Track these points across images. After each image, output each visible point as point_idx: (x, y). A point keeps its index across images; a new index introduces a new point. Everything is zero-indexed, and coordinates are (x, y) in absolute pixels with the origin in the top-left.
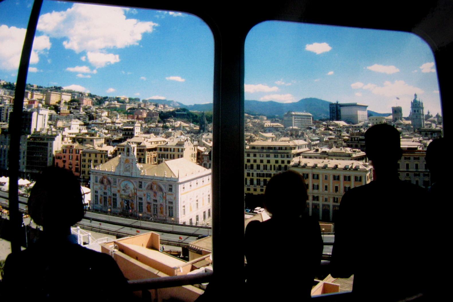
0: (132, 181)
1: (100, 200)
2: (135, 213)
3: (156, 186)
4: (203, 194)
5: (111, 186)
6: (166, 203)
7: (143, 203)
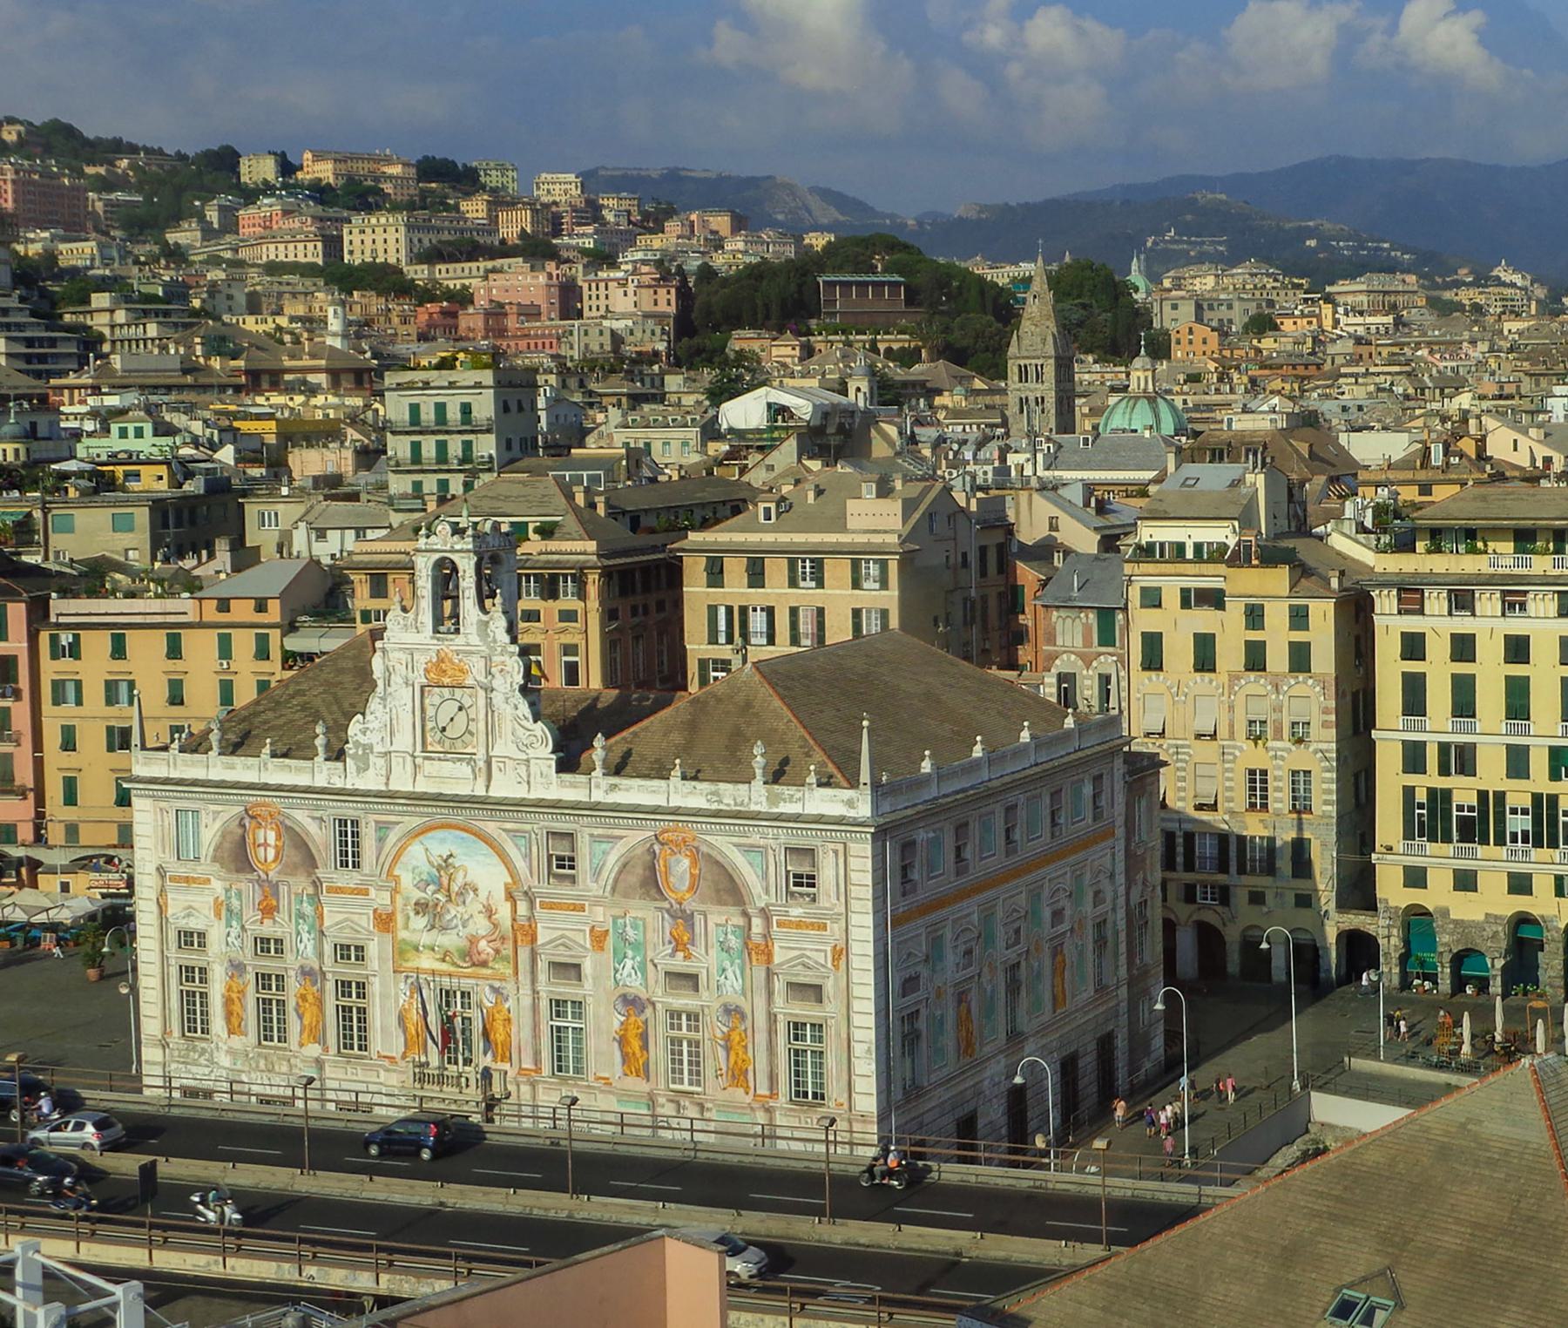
0: (491, 828)
1: (228, 1001)
2: (525, 1089)
3: (686, 862)
4: (1057, 915)
5: (317, 884)
6: (770, 994)
7: (590, 1009)
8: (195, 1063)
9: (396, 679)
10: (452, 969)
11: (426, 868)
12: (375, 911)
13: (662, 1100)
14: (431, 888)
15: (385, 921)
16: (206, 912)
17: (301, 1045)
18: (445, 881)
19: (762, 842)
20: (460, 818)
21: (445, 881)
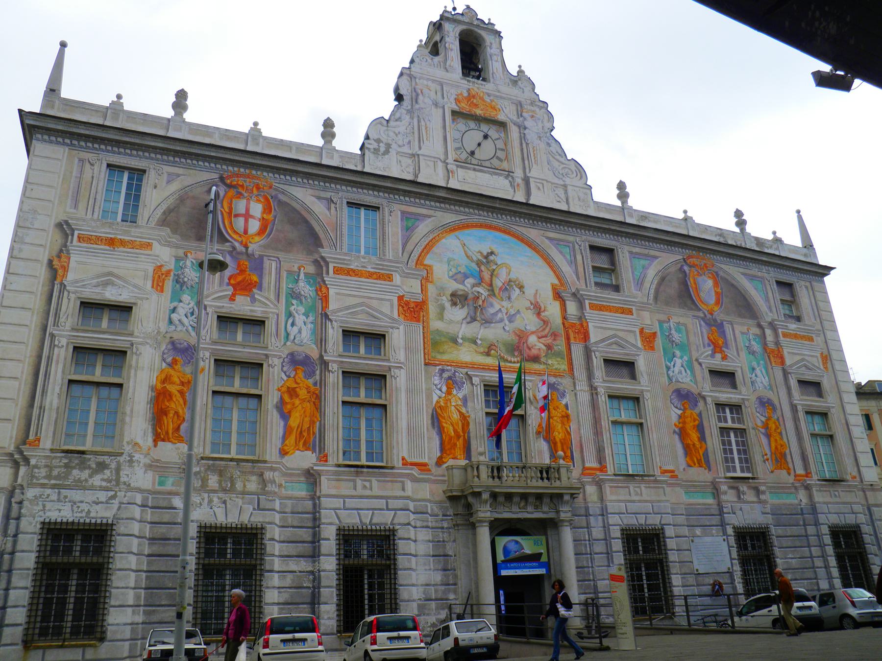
0: (534, 233)
2: (591, 490)
3: (710, 283)
5: (321, 264)
6: (789, 389)
7: (649, 403)
8: (79, 485)
9: (424, 101)
11: (465, 261)
12: (400, 298)
13: (724, 488)
14: (470, 281)
16: (140, 282)
17: (283, 453)
18: (486, 276)
19: (759, 274)
20: (500, 221)
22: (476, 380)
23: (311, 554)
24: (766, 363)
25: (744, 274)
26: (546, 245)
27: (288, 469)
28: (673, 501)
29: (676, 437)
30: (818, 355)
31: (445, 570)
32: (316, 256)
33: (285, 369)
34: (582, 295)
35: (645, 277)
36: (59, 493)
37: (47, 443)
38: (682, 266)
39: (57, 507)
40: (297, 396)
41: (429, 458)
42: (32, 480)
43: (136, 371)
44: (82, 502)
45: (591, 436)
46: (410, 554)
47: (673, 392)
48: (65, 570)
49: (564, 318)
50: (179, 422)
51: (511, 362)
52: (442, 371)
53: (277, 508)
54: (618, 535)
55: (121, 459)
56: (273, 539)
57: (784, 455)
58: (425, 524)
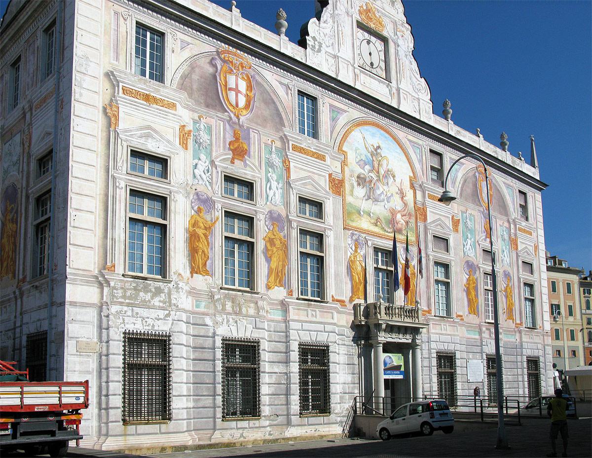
8: (145, 305)
10: (382, 232)
11: (364, 152)
12: (330, 175)
13: (484, 329)
14: (367, 167)
15: (337, 186)
17: (268, 287)
18: (376, 166)
21: (376, 166)
22: (370, 243)
23: (285, 361)
24: (509, 247)
25: (504, 183)
26: (408, 145)
27: (271, 299)
28: (460, 336)
29: (465, 293)
30: (533, 245)
31: (353, 374)
32: (281, 134)
33: (267, 223)
34: (425, 187)
35: (457, 177)
36: (132, 309)
37: (120, 270)
38: (475, 172)
39: (132, 321)
40: (275, 245)
41: (346, 297)
42: (113, 299)
43: (175, 215)
44: (148, 318)
45: (425, 290)
46: (336, 363)
47: (465, 263)
48: (139, 367)
49: (415, 203)
50: (206, 259)
51: (387, 232)
52: (353, 234)
53: (266, 328)
54: (435, 355)
55: (170, 285)
56: (264, 350)
57: (512, 310)
58: (343, 342)
